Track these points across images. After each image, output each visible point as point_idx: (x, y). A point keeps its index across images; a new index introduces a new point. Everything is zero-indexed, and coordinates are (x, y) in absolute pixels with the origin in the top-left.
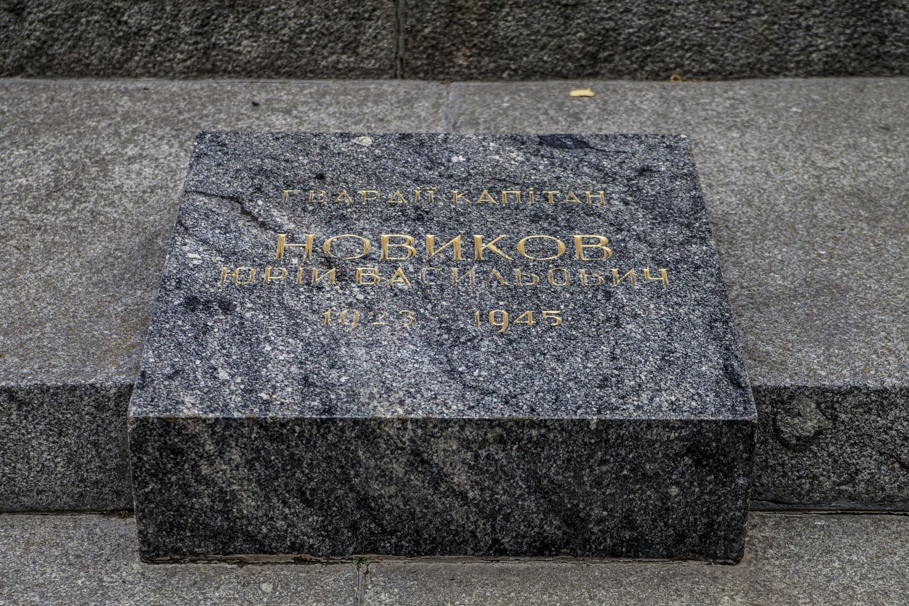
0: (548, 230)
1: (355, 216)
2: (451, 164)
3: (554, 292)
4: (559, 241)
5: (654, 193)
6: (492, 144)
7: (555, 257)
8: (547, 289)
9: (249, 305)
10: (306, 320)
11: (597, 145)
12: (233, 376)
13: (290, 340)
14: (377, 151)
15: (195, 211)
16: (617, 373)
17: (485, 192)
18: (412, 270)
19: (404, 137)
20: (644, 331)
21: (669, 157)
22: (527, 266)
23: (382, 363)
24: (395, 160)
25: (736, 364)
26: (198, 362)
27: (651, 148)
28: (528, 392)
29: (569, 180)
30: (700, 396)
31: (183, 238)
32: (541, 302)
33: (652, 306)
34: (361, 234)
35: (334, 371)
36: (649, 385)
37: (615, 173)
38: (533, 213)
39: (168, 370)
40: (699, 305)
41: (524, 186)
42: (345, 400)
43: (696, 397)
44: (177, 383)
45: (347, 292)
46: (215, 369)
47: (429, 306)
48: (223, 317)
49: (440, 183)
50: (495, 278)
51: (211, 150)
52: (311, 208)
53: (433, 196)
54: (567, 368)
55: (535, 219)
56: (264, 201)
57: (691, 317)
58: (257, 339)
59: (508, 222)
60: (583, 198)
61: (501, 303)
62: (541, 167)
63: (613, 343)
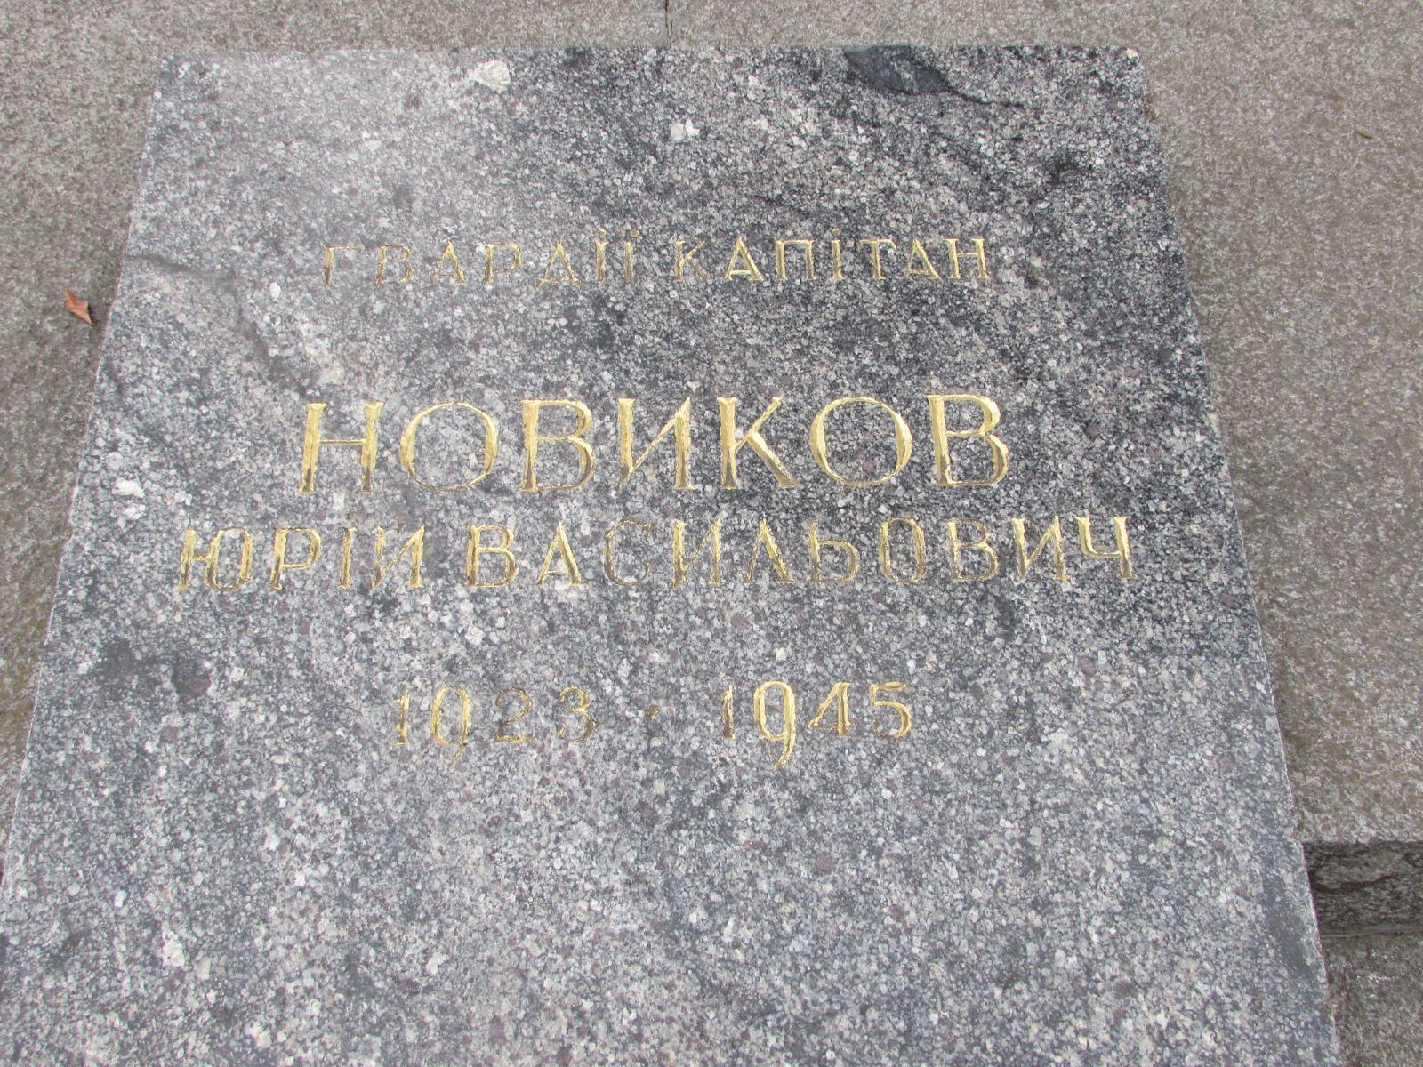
0: (872, 377)
1: (469, 335)
2: (670, 148)
3: (893, 608)
4: (898, 418)
5: (1084, 243)
6: (753, 81)
7: (889, 478)
8: (879, 598)
9: (237, 674)
10: (357, 729)
11: (963, 80)
12: (192, 952)
13: (321, 810)
14: (520, 108)
15: (143, 324)
16: (1037, 922)
17: (740, 244)
18: (586, 530)
19: (578, 57)
20: (1088, 757)
21: (1112, 125)
22: (833, 511)
23: (519, 899)
24: (557, 135)
25: (1289, 880)
26: (120, 897)
27: (1071, 92)
28: (844, 1008)
29: (914, 199)
30: (1220, 1007)
31: (111, 421)
32: (866, 645)
33: (1102, 658)
34: (479, 400)
35: (414, 931)
36: (1108, 970)
37: (1004, 176)
38: (841, 312)
39: (55, 934)
40: (1199, 650)
41: (822, 221)
42: (437, 1047)
43: (1211, 1013)
44: (70, 983)
45: (446, 620)
46: (156, 927)
47: (624, 670)
48: (178, 721)
49: (647, 212)
50: (766, 562)
51: (186, 117)
52: (379, 307)
53: (633, 261)
54: (929, 905)
55: (846, 337)
56: (284, 286)
57: (1186, 696)
58: (249, 806)
59: (790, 348)
60: (942, 260)
61: (780, 654)
62: (853, 157)
63: (1024, 799)
